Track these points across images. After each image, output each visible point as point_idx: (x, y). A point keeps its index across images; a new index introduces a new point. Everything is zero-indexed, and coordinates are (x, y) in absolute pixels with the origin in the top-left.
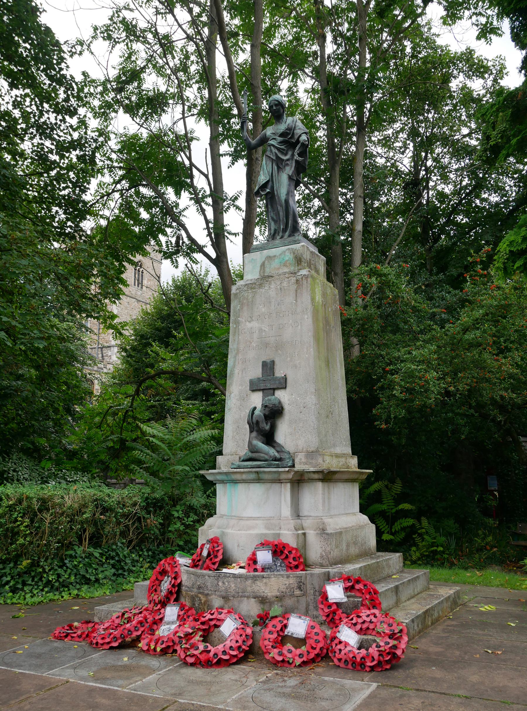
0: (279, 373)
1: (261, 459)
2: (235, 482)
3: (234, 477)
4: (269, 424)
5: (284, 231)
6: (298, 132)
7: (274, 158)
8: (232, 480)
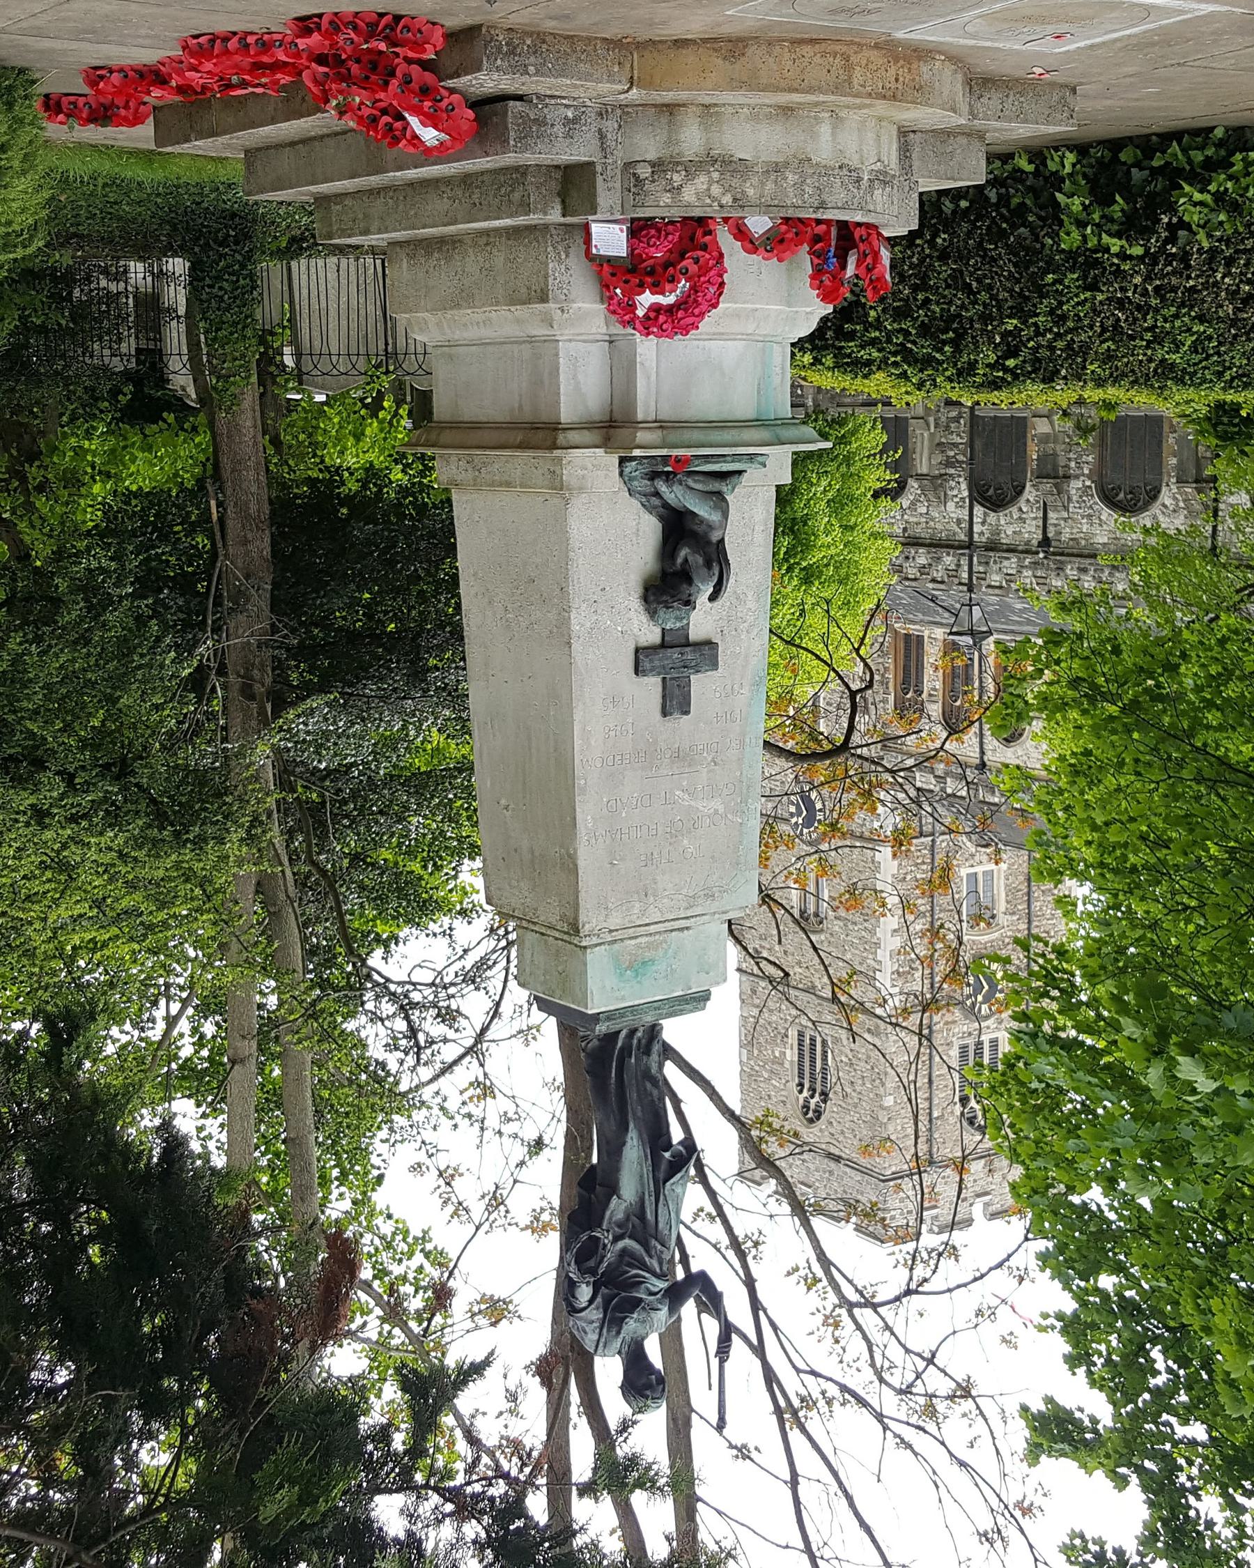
2: (759, 422)
3: (764, 434)
4: (679, 561)
5: (626, 1051)
6: (595, 1314)
7: (653, 1242)
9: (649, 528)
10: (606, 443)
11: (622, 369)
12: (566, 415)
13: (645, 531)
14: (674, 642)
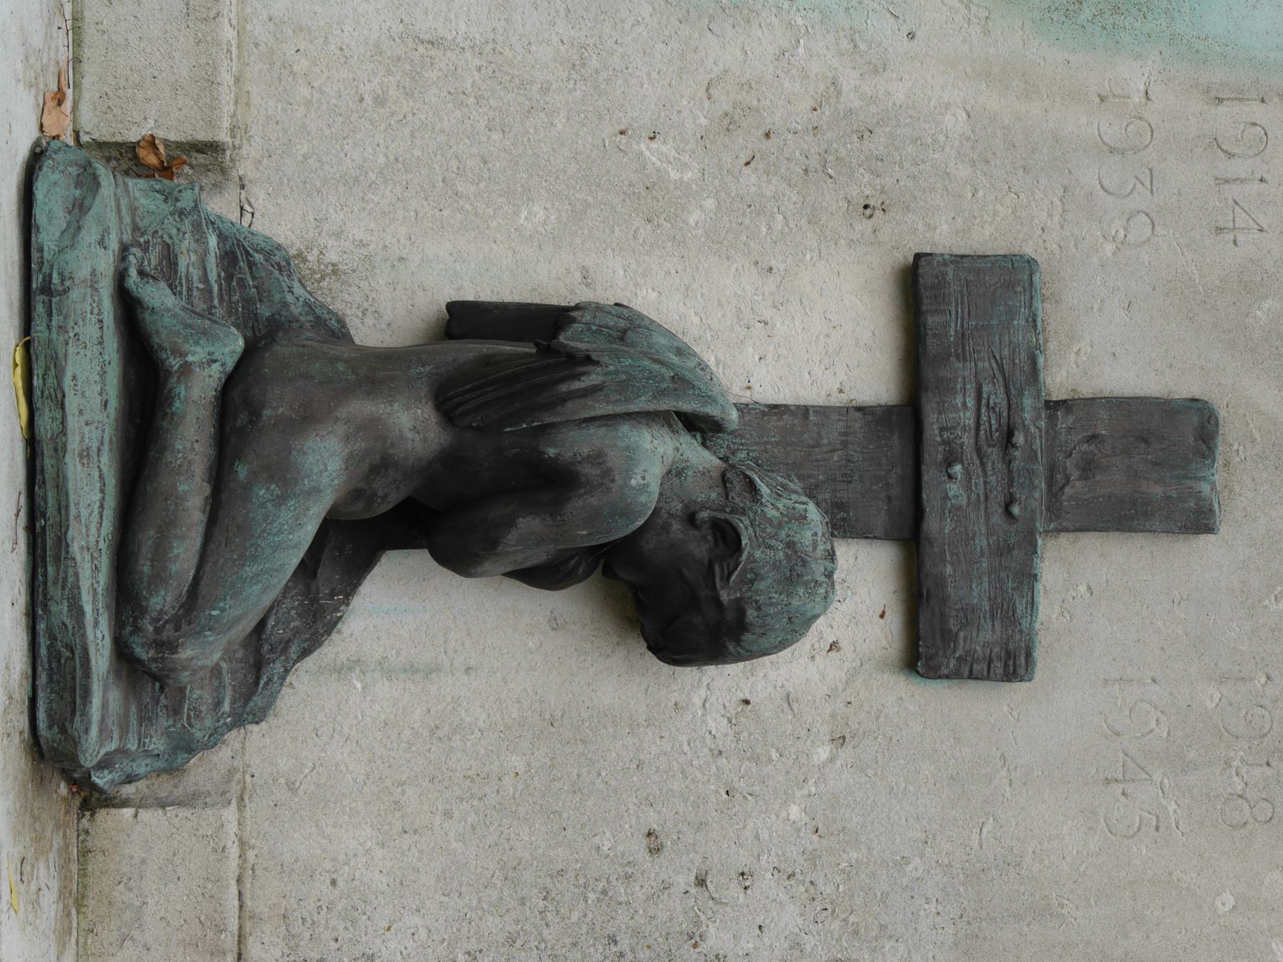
0: (1086, 585)
1: (147, 539)
9: (401, 604)
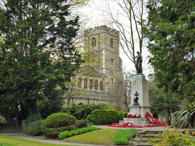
0: (138, 93)
2: (132, 108)
8: (131, 107)
9: (138, 102)
10: (140, 107)
11: (140, 111)
12: (143, 108)
13: (138, 102)
14: (137, 96)
